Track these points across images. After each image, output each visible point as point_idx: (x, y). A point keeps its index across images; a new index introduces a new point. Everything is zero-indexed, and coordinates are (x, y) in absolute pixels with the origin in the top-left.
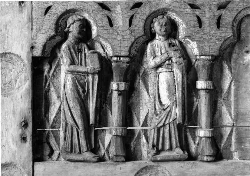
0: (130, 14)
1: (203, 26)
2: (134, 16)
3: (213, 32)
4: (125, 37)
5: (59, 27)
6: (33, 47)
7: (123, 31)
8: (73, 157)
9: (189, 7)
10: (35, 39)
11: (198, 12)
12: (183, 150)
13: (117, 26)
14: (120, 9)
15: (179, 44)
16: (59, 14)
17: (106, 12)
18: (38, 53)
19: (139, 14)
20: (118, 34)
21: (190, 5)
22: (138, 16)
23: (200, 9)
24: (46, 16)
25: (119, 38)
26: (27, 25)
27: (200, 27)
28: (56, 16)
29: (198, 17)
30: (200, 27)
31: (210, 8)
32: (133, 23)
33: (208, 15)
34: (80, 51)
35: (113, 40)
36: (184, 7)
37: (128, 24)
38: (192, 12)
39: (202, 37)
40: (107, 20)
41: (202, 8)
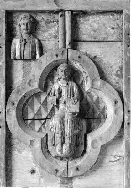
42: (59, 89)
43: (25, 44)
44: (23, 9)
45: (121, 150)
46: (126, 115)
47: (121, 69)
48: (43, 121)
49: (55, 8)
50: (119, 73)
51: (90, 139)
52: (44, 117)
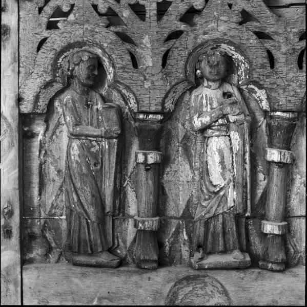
0: (164, 49)
1: (277, 66)
2: (171, 52)
3: (291, 75)
4: (156, 84)
5: (59, 68)
7: (153, 75)
9: (255, 37)
10: (22, 86)
11: (268, 44)
12: (242, 251)
13: (144, 67)
14: (148, 40)
15: (239, 95)
16: (58, 50)
17: (128, 46)
18: (26, 108)
19: (177, 48)
20: (145, 79)
21: (256, 33)
22: (176, 52)
23: (272, 39)
24: (40, 52)
25: (147, 85)
26: (11, 67)
27: (272, 66)
28: (53, 52)
29: (269, 52)
30: (272, 66)
31: (287, 39)
32: (168, 62)
33: (284, 49)
35: (139, 88)
36: (246, 37)
37: (160, 63)
38: (259, 45)
39: (274, 83)
40: (130, 58)
41: (276, 37)
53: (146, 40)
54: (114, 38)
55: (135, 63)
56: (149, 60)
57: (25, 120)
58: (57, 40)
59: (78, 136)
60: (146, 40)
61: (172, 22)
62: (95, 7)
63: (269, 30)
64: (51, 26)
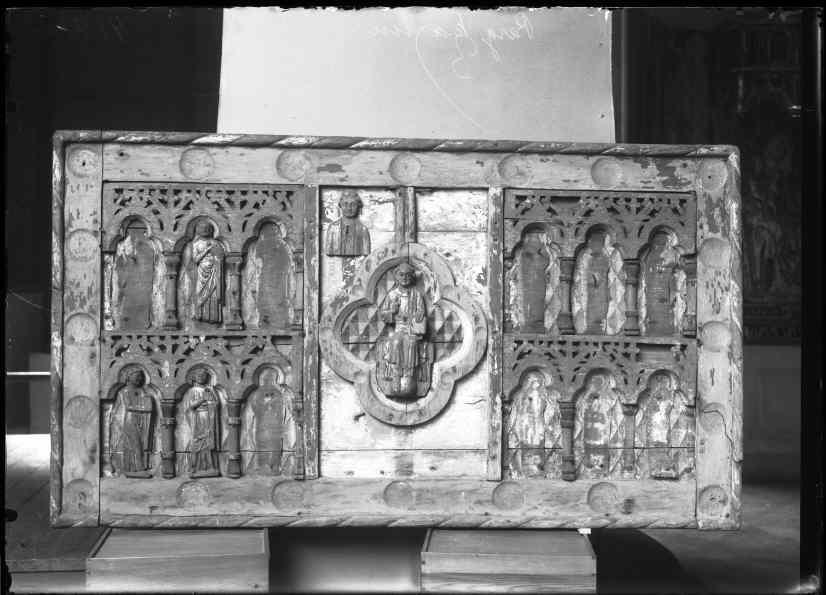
6: (100, 392)
8: (132, 474)
12: (214, 467)
17: (157, 366)
18: (104, 396)
25: (167, 386)
33: (234, 369)
34: (137, 394)
42: (397, 300)
43: (347, 233)
44: (344, 183)
45: (480, 385)
46: (490, 337)
47: (485, 271)
48: (371, 346)
49: (391, 182)
50: (482, 278)
51: (436, 366)
52: (372, 339)
53: (167, 363)
54: (150, 362)
55: (160, 374)
56: (167, 372)
57: (102, 402)
58: (121, 362)
59: (131, 411)
60: (167, 363)
61: (180, 353)
62: (141, 346)
63: (227, 360)
64: (118, 354)
